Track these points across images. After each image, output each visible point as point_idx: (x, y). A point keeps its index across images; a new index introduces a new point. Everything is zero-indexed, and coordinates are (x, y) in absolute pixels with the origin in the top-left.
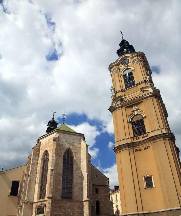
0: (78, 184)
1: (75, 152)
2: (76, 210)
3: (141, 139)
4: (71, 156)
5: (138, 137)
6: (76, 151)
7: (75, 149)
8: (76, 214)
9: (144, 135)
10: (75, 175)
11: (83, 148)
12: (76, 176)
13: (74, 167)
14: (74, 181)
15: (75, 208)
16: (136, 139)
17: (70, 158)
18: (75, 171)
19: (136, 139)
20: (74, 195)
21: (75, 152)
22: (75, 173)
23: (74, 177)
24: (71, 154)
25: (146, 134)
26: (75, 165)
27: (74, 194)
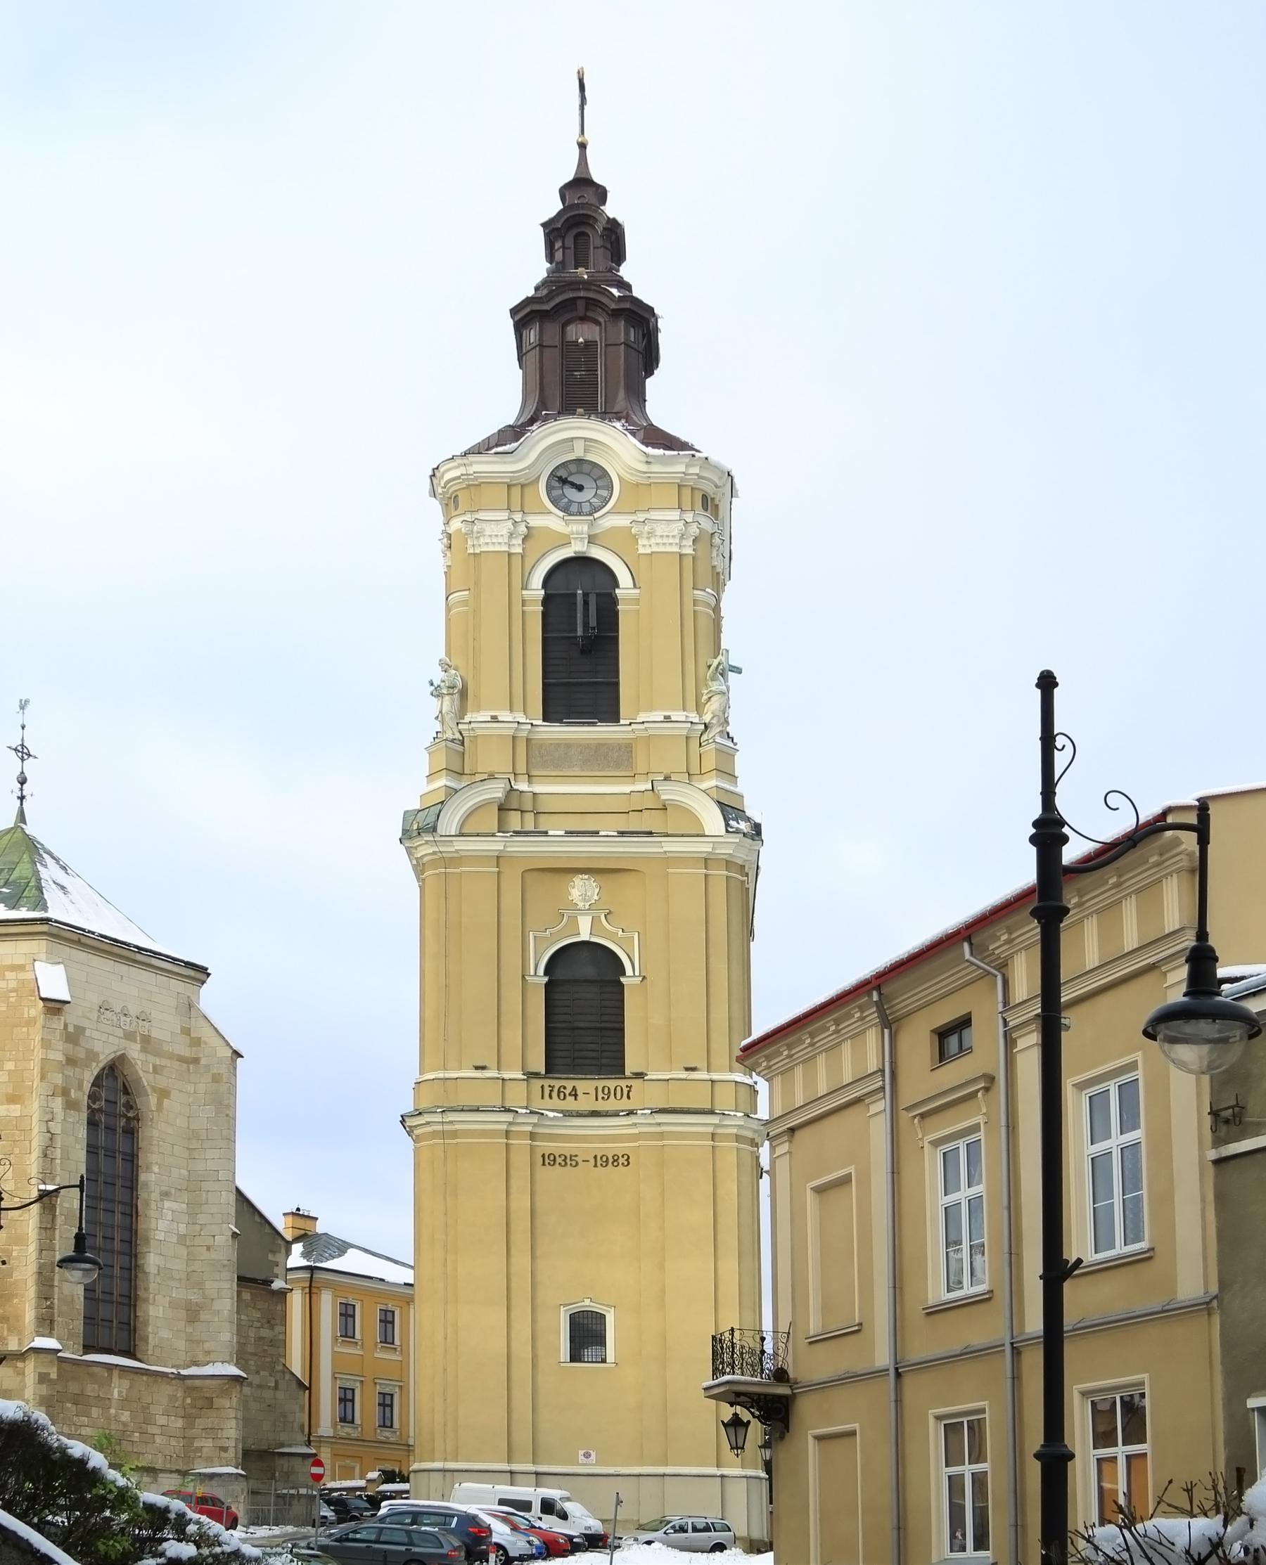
0: (172, 1278)
1: (154, 1089)
2: (161, 1420)
3: (585, 1104)
4: (129, 1106)
5: (569, 1085)
6: (161, 1082)
7: (155, 1067)
8: (158, 1439)
9: (612, 1084)
10: (153, 1226)
11: (208, 1066)
12: (161, 1236)
13: (152, 1177)
14: (152, 1261)
15: (157, 1410)
16: (555, 1094)
17: (123, 1122)
18: (153, 1205)
19: (555, 1094)
20: (152, 1341)
21: (154, 1089)
22: (153, 1214)
23: (147, 1240)
24: (126, 1091)
25: (623, 1083)
26: (156, 1169)
27: (151, 1336)
